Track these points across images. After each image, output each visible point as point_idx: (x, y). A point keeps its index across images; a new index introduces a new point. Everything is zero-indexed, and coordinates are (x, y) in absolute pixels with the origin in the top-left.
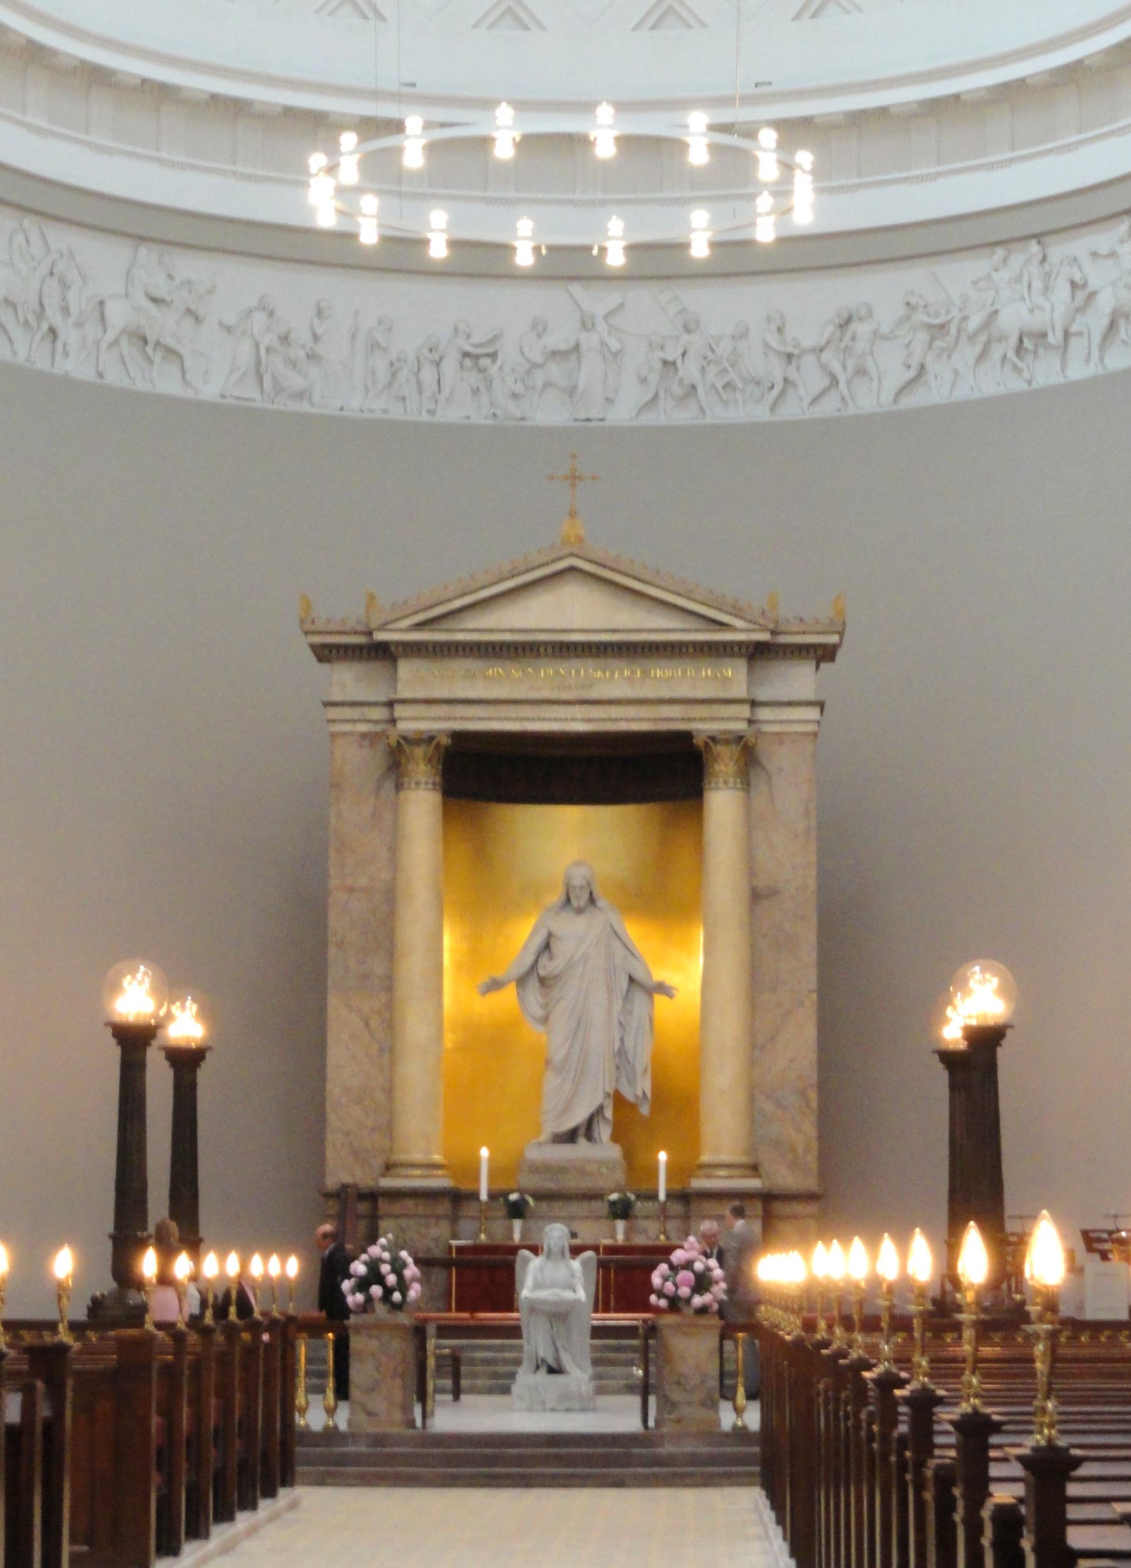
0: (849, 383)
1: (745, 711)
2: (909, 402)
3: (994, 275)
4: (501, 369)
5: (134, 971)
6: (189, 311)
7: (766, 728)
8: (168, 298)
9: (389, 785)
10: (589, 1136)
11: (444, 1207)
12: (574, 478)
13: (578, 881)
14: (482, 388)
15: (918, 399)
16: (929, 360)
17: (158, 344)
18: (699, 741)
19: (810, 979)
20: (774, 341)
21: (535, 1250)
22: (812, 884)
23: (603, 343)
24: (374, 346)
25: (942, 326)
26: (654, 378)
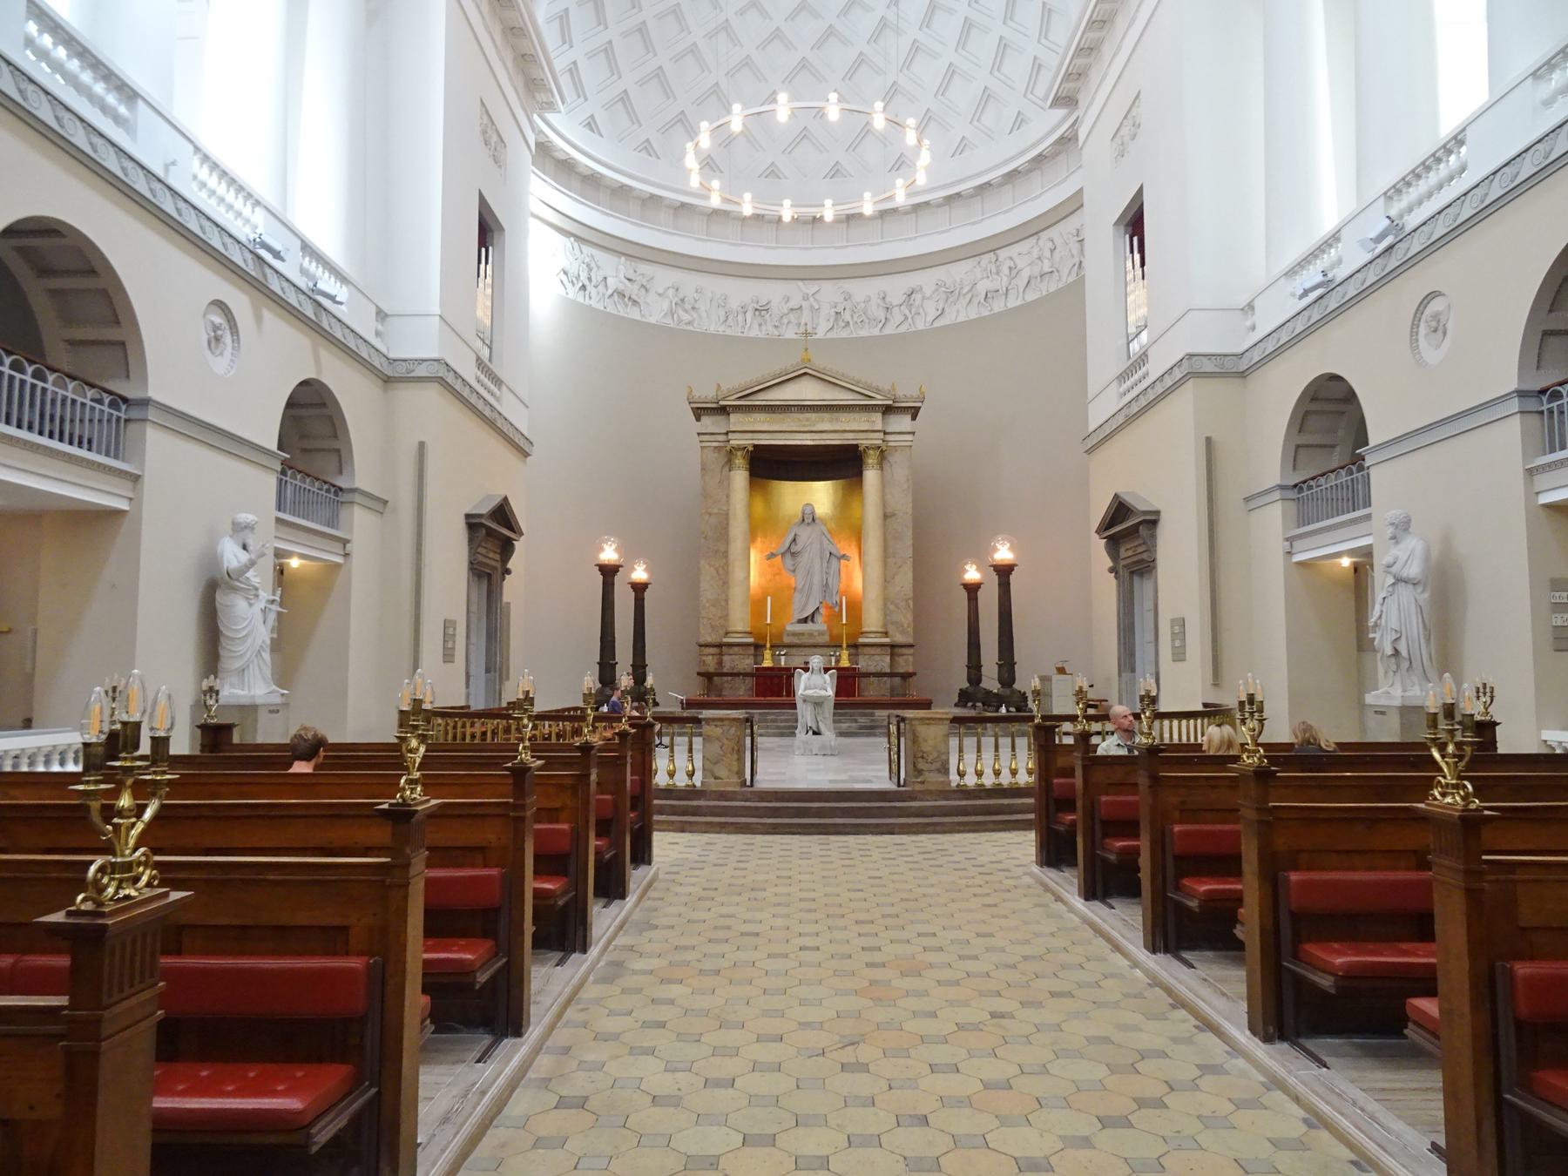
0: (912, 318)
1: (881, 435)
2: (937, 324)
6: (643, 286)
7: (890, 444)
9: (727, 468)
10: (813, 621)
13: (808, 511)
17: (630, 298)
18: (861, 448)
19: (910, 553)
21: (806, 670)
22: (910, 511)
23: (812, 306)
26: (832, 320)
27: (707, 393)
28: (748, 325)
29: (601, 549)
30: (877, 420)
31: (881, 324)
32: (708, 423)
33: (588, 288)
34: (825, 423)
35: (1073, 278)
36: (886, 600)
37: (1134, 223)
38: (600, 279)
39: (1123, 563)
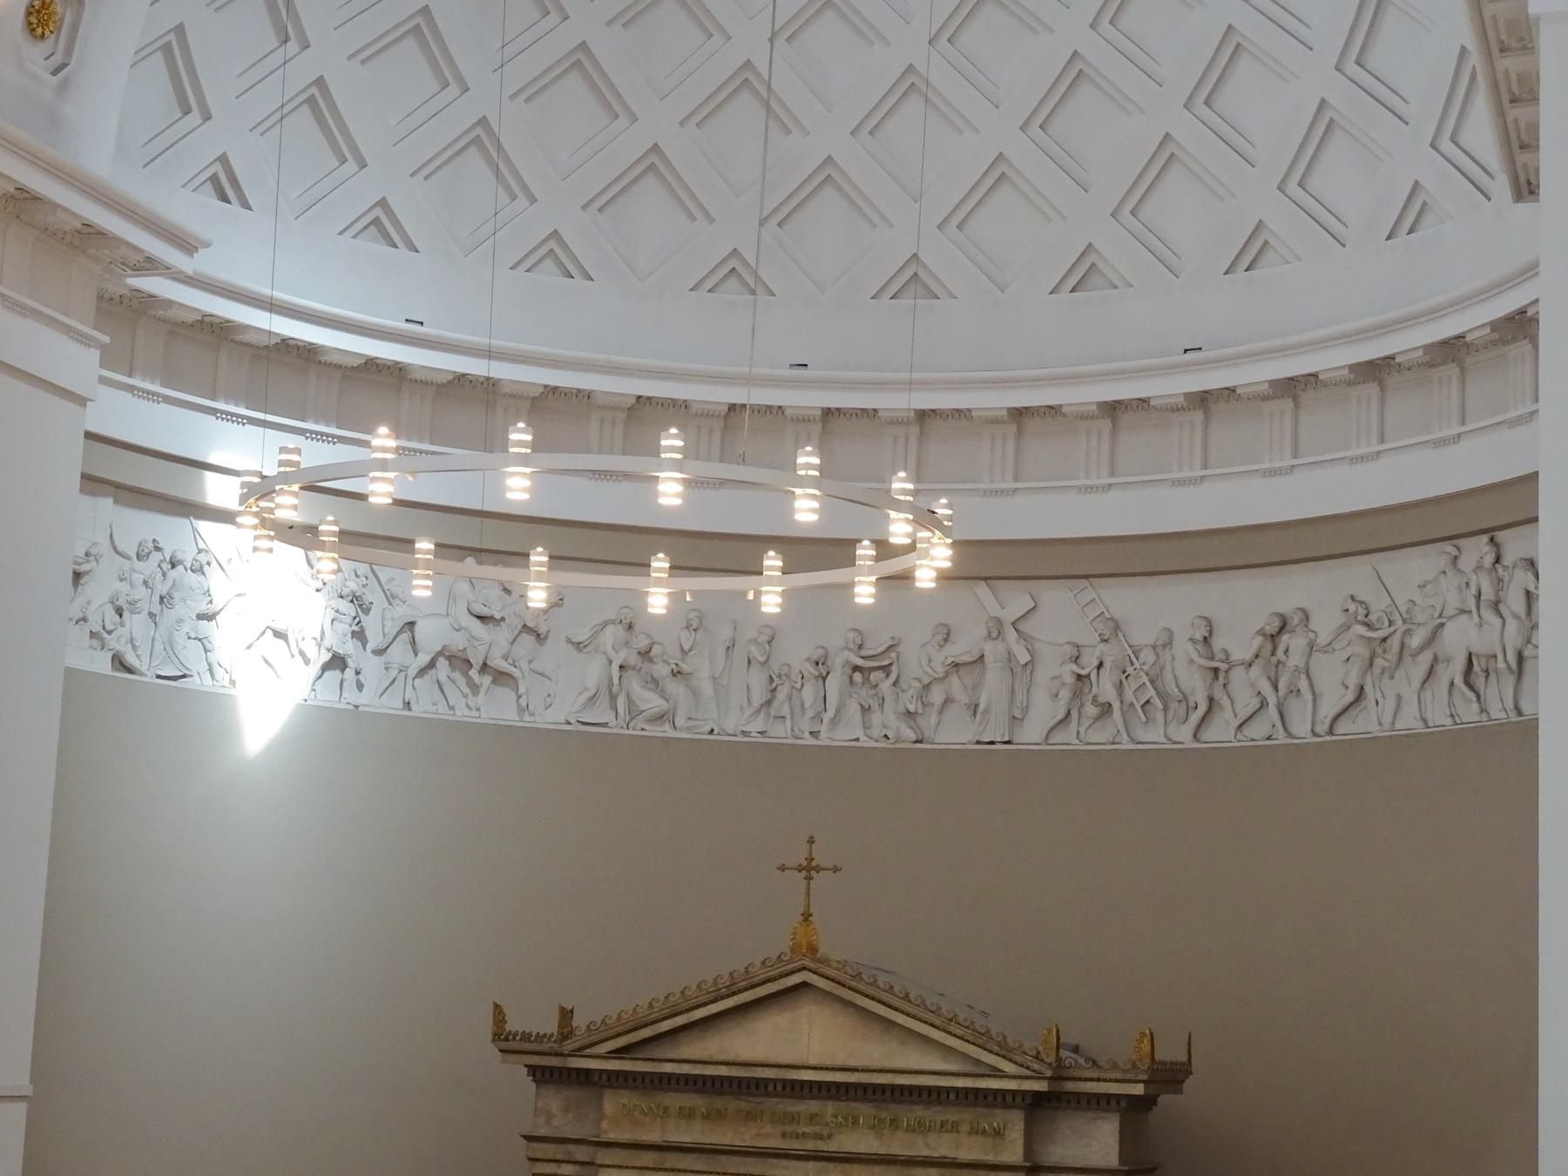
3: (1442, 579)
4: (895, 684)
8: (498, 616)
12: (809, 869)
14: (875, 705)
17: (485, 668)
23: (1010, 656)
25: (1384, 640)
26: (1065, 694)
28: (831, 713)
31: (1195, 717)
33: (350, 662)
38: (392, 629)
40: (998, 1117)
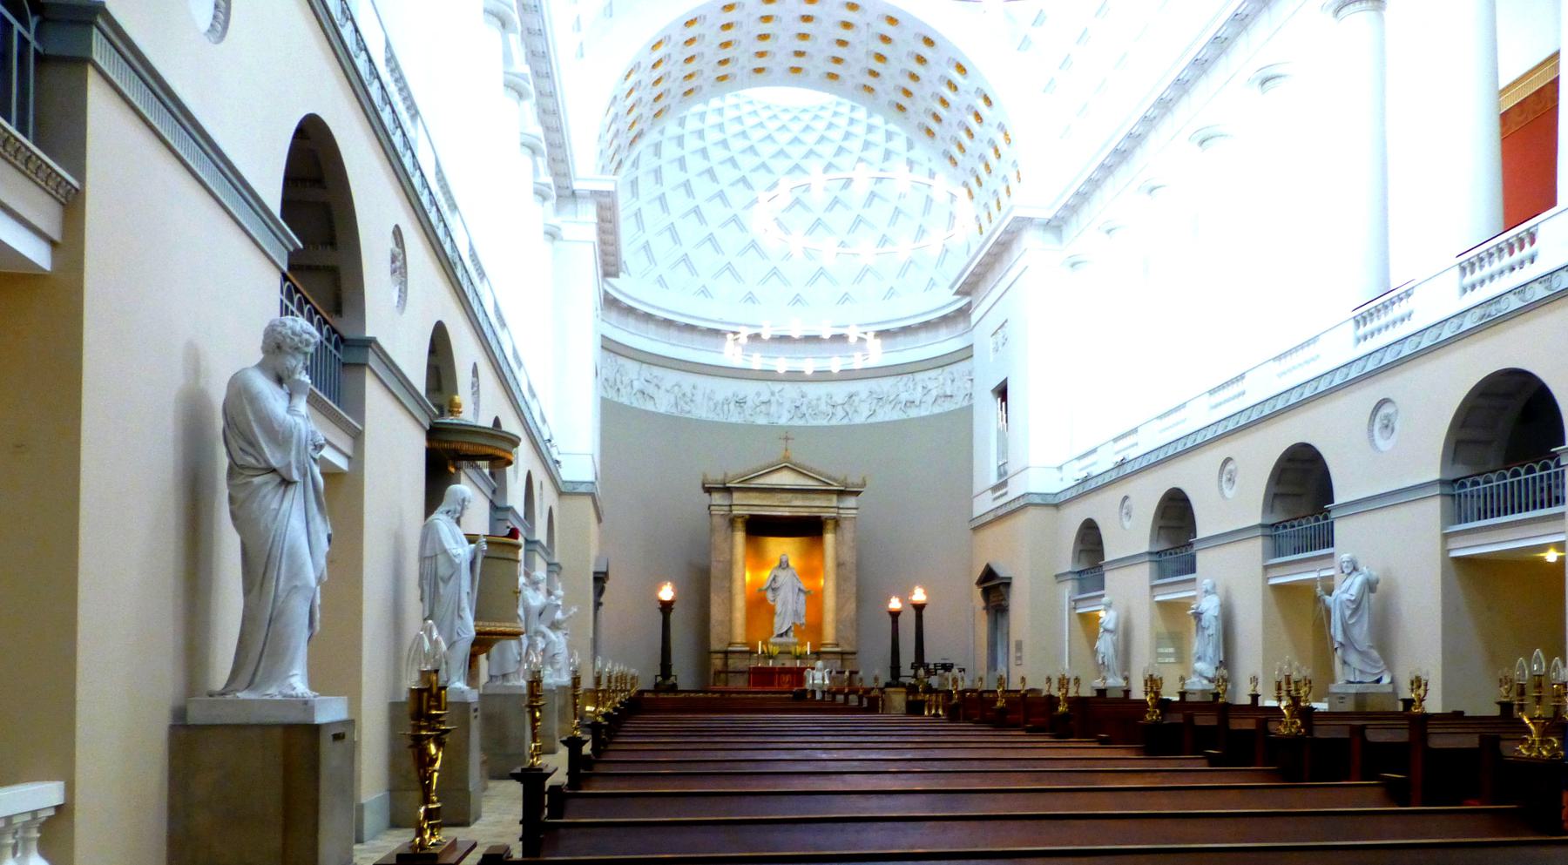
1: (836, 510)
2: (870, 421)
5: (666, 584)
7: (843, 516)
9: (730, 530)
11: (748, 656)
12: (787, 439)
13: (784, 560)
15: (872, 420)
16: (877, 408)
17: (648, 395)
18: (823, 518)
20: (829, 401)
22: (855, 562)
23: (778, 401)
24: (710, 399)
26: (793, 411)
27: (716, 476)
29: (660, 589)
30: (834, 501)
32: (717, 498)
34: (798, 501)
35: (965, 404)
36: (838, 622)
37: (1002, 392)
39: (993, 604)
40: (830, 496)
